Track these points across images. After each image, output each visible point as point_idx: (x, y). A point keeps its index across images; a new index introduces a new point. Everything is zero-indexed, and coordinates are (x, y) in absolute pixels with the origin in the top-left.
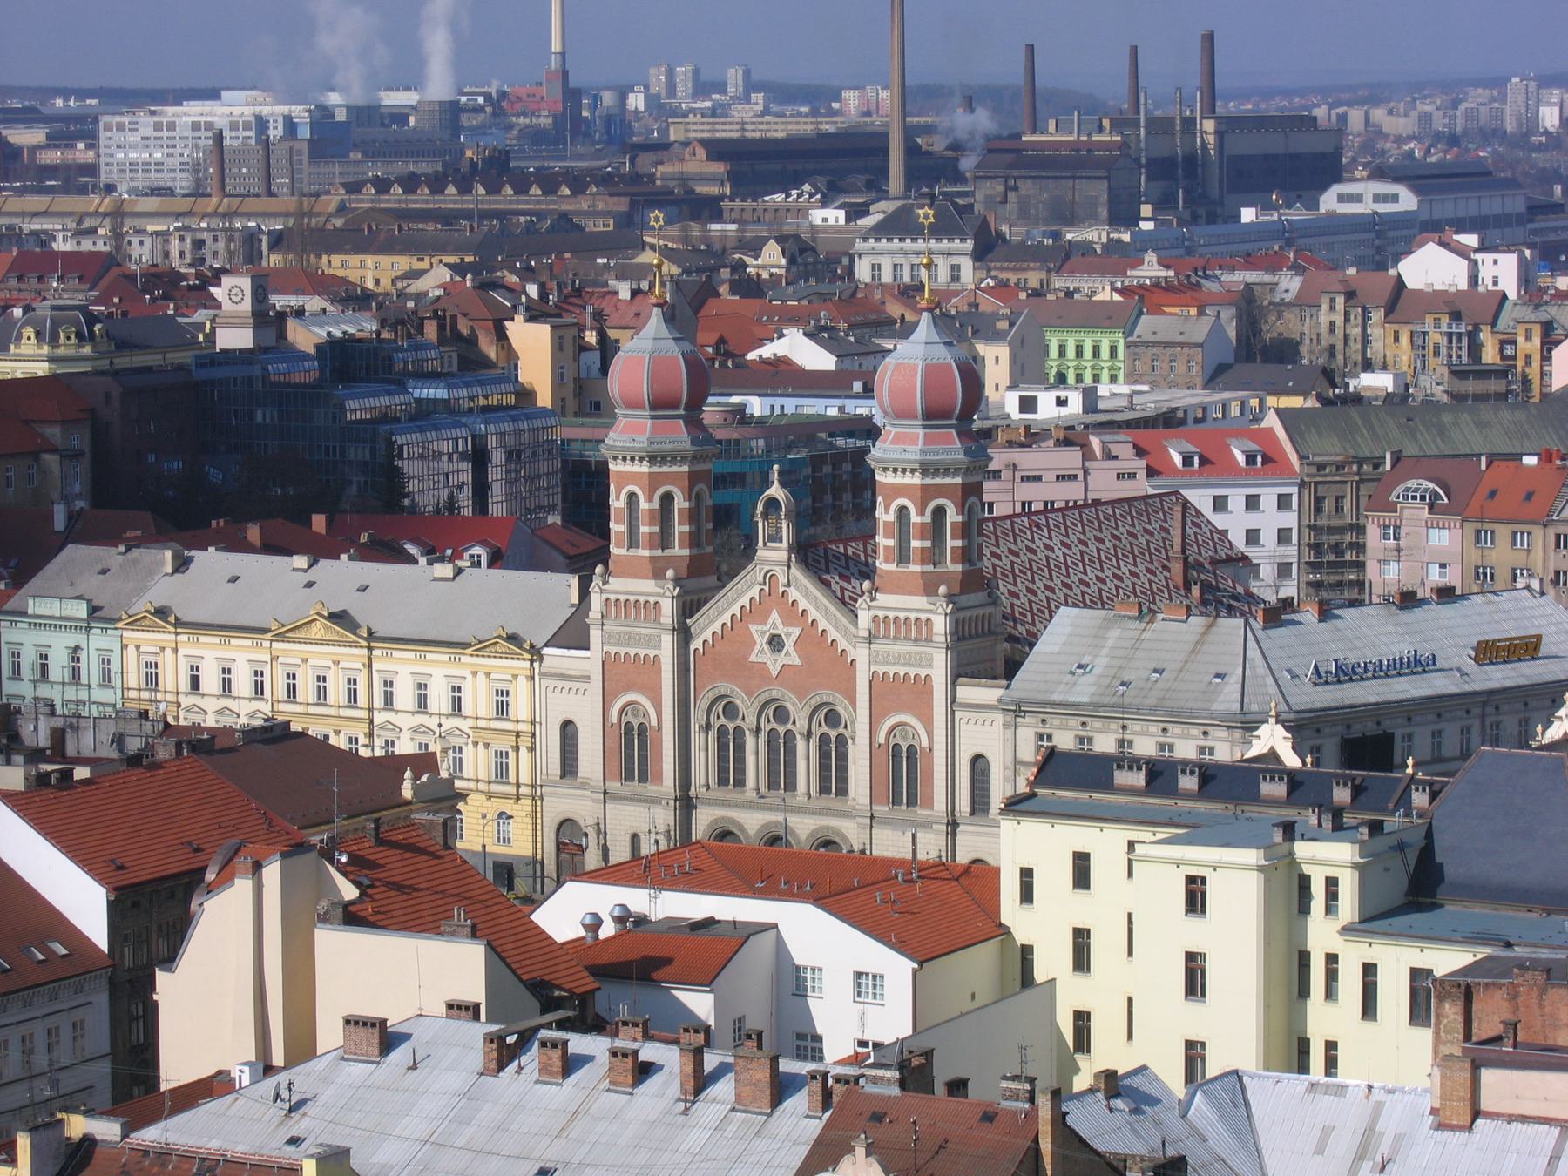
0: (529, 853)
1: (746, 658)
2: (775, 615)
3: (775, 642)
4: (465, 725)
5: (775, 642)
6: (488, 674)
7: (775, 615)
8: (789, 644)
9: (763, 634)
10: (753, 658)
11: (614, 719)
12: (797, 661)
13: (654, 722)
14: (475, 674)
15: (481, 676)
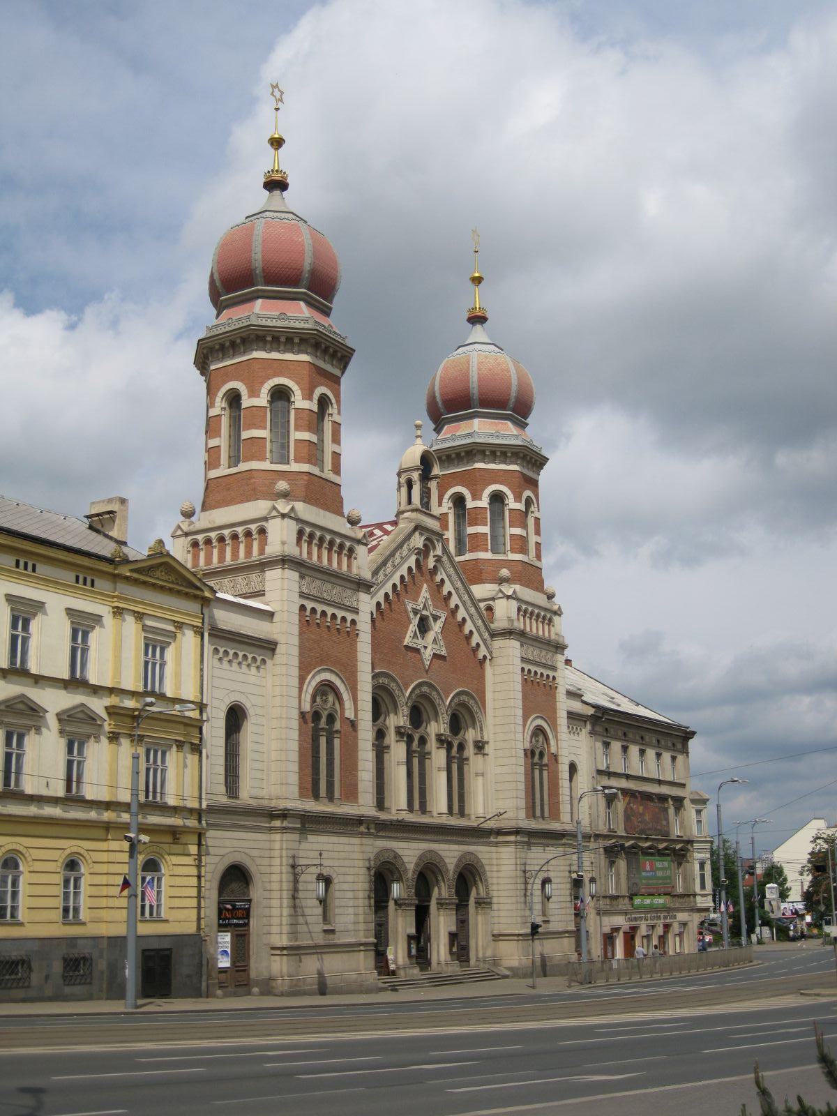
0: (191, 928)
1: (402, 642)
2: (425, 593)
3: (423, 627)
4: (98, 705)
5: (423, 627)
6: (139, 616)
7: (425, 593)
8: (437, 627)
9: (415, 612)
10: (407, 641)
11: (307, 707)
12: (444, 652)
13: (349, 713)
14: (118, 612)
15: (130, 619)
